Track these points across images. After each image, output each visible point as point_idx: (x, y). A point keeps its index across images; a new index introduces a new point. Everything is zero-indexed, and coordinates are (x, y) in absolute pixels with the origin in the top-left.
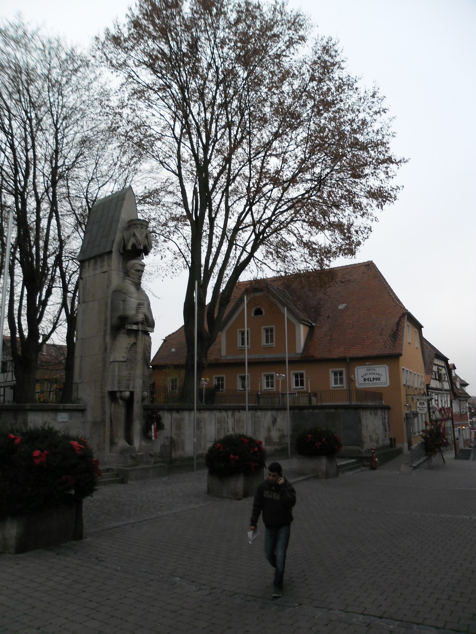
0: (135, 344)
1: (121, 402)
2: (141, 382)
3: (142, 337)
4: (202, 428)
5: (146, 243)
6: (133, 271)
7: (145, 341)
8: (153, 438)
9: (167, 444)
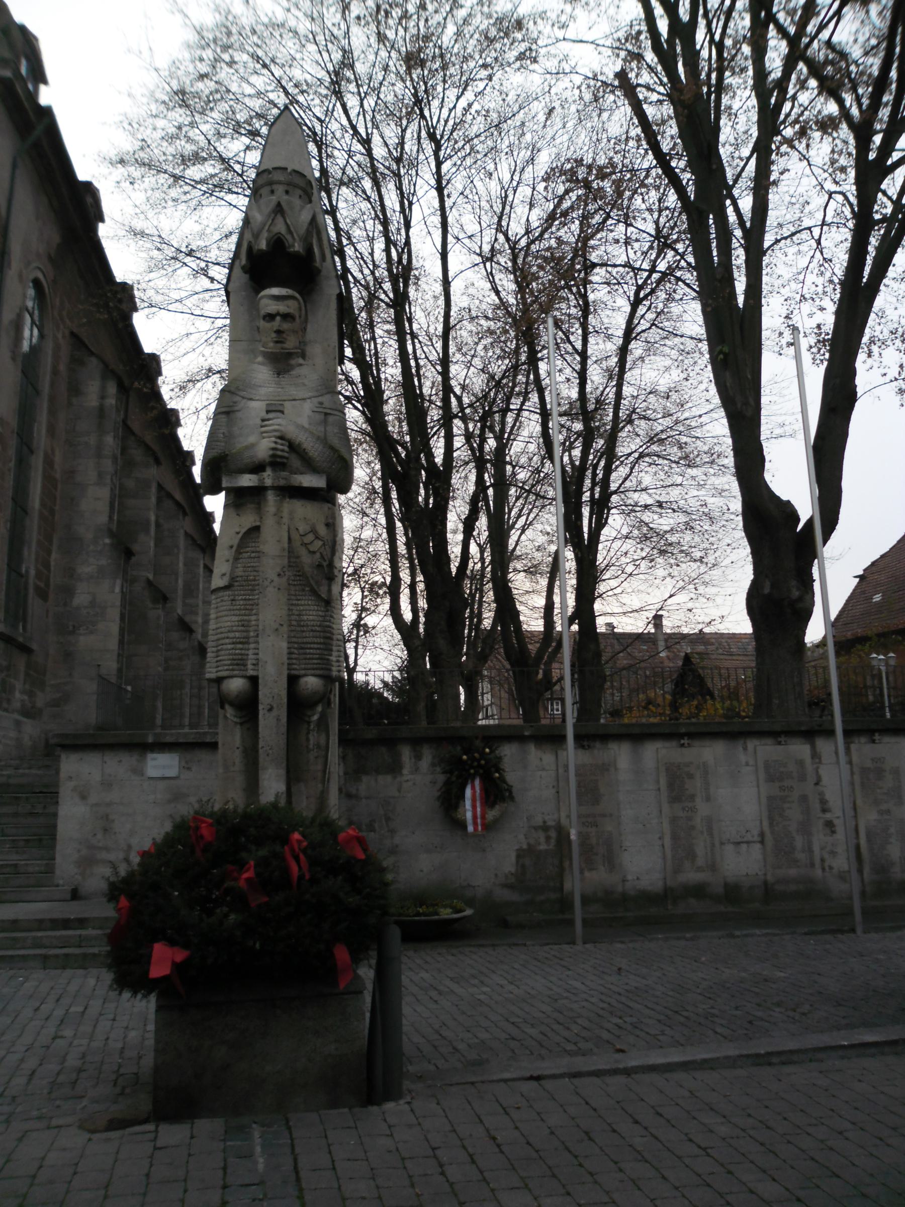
1: (230, 711)
2: (285, 645)
4: (692, 797)
5: (280, 227)
6: (262, 324)
8: (470, 829)
9: (543, 847)
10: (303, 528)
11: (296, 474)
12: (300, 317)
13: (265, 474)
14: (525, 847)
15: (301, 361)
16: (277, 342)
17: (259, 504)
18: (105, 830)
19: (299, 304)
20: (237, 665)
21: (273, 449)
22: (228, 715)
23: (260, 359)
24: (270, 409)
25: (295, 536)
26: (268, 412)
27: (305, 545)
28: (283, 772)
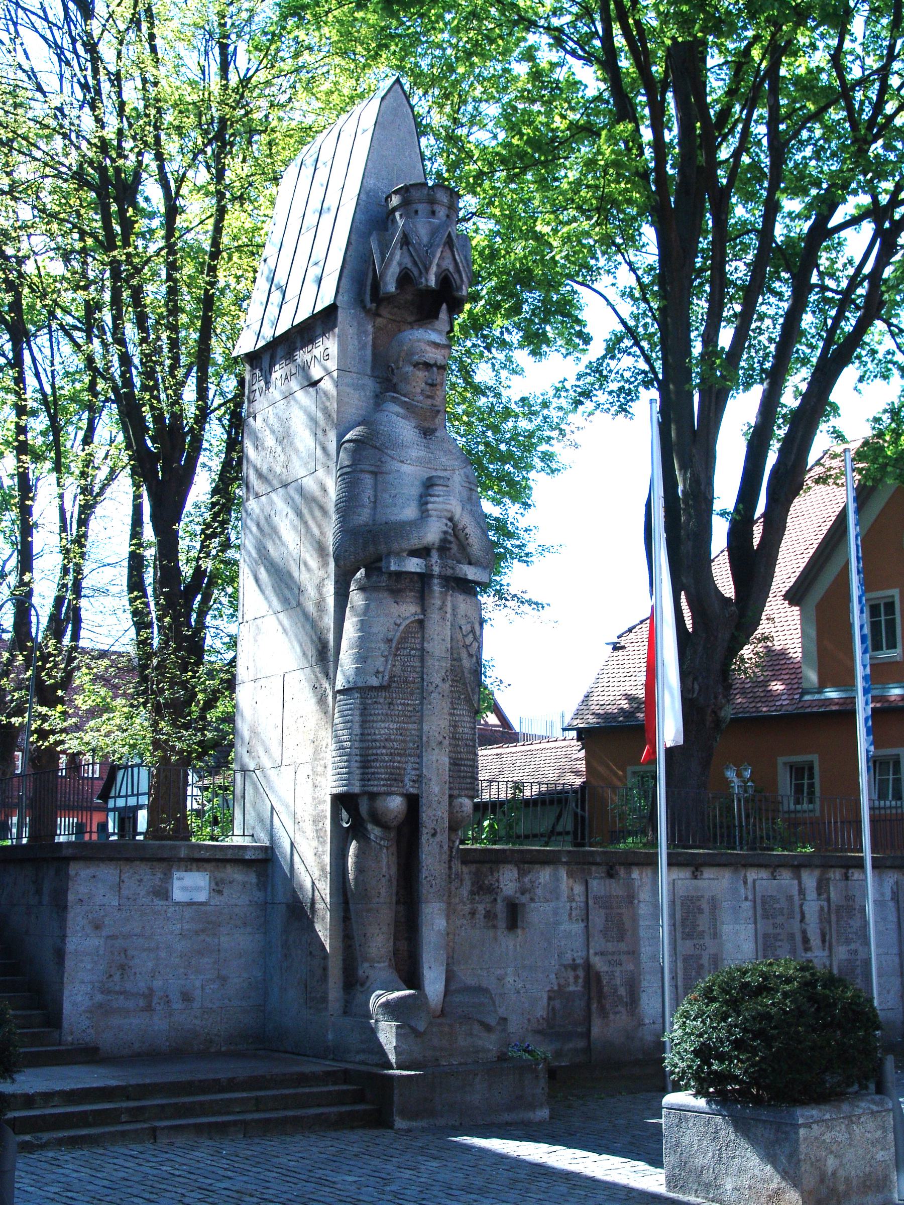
2: (447, 760)
5: (448, 264)
7: (454, 615)
9: (572, 988)
10: (466, 628)
14: (556, 988)
16: (428, 397)
18: (122, 967)
20: (395, 780)
22: (372, 837)
27: (467, 647)
28: (443, 906)
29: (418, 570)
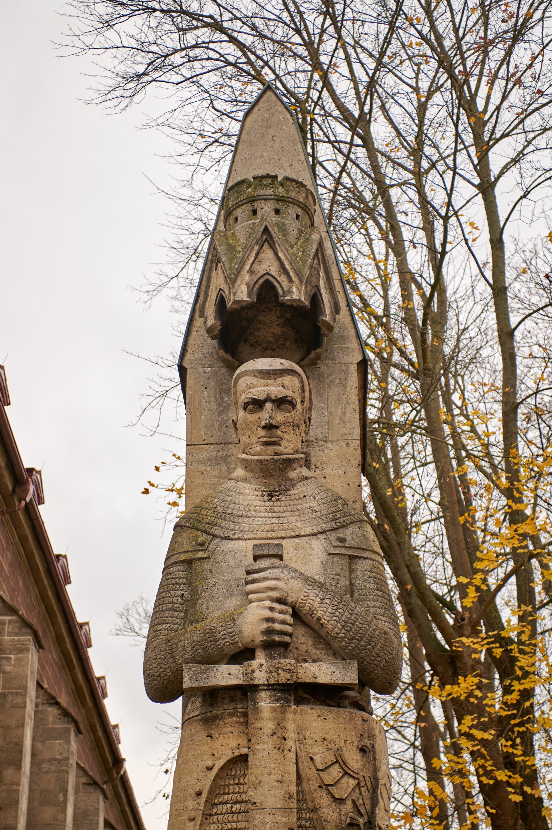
0: (243, 759)
3: (280, 725)
11: (305, 661)
12: (303, 402)
13: (255, 664)
15: (305, 472)
16: (267, 444)
17: (245, 715)
19: (302, 381)
21: (268, 620)
23: (240, 472)
24: (259, 553)
25: (309, 772)
26: (256, 558)
29: (232, 682)
